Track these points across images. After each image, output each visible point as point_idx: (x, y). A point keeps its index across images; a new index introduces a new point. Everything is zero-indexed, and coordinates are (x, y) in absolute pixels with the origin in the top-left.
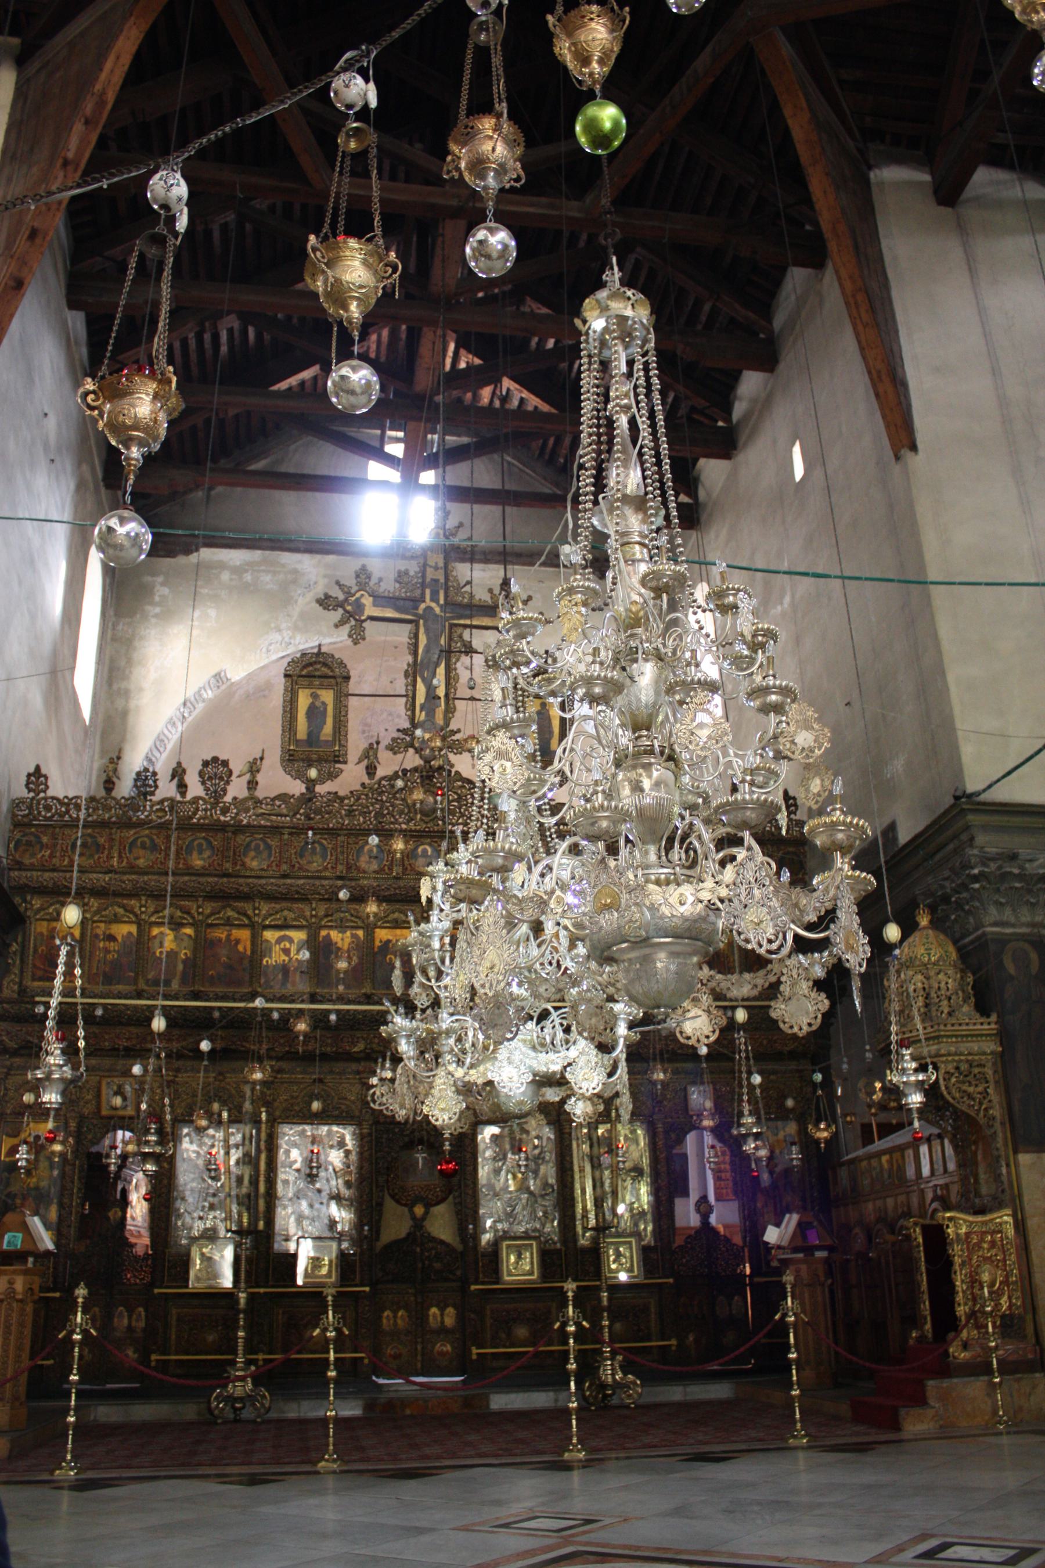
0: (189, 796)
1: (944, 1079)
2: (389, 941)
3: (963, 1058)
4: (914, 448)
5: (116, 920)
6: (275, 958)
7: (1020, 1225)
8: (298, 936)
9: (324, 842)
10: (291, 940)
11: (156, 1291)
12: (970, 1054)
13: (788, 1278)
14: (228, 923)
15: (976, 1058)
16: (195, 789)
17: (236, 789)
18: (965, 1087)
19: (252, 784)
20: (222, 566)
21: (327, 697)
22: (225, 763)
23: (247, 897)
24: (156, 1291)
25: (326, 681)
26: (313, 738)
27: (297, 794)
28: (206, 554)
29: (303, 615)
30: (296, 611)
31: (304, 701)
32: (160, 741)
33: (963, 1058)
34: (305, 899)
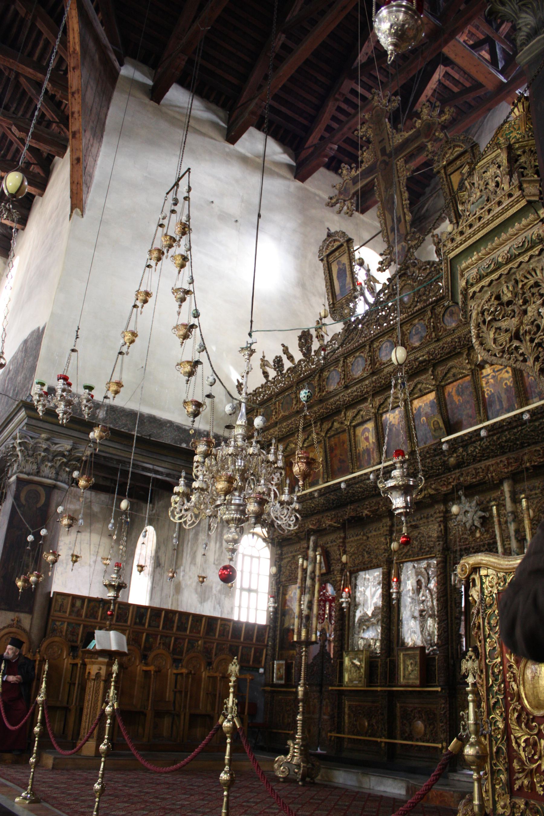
0: (296, 361)
1: (478, 325)
2: (420, 407)
3: (495, 276)
9: (362, 354)
10: (367, 430)
11: (330, 688)
12: (499, 266)
13: (234, 666)
15: (514, 264)
17: (315, 345)
18: (504, 324)
19: (320, 337)
23: (337, 411)
24: (330, 688)
25: (341, 250)
27: (341, 331)
33: (495, 276)
34: (365, 400)
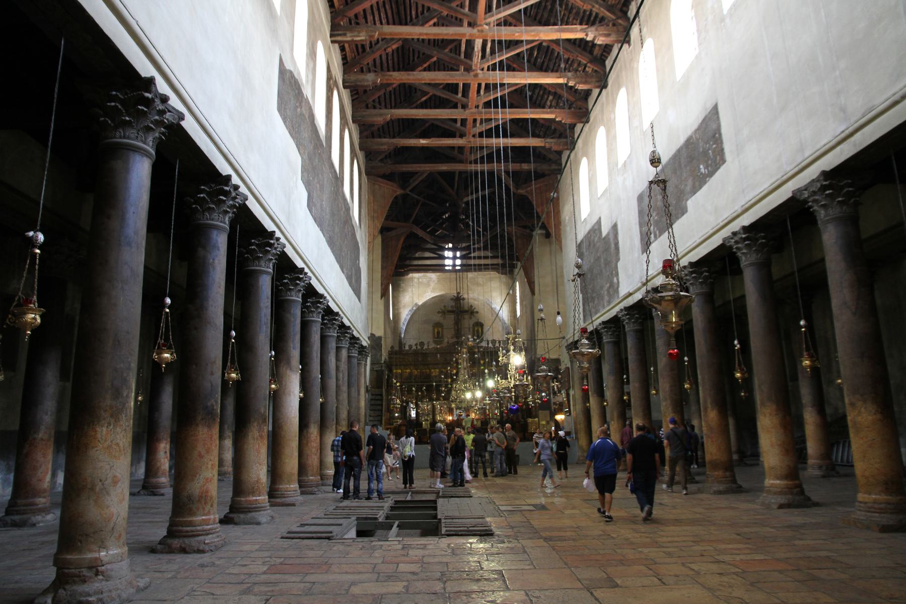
4: (534, 295)
5: (407, 369)
6: (434, 374)
7: (539, 421)
8: (437, 370)
14: (425, 369)
16: (419, 347)
17: (425, 347)
20: (415, 278)
21: (440, 329)
26: (438, 337)
28: (411, 275)
29: (433, 288)
30: (431, 287)
31: (436, 331)
32: (405, 319)
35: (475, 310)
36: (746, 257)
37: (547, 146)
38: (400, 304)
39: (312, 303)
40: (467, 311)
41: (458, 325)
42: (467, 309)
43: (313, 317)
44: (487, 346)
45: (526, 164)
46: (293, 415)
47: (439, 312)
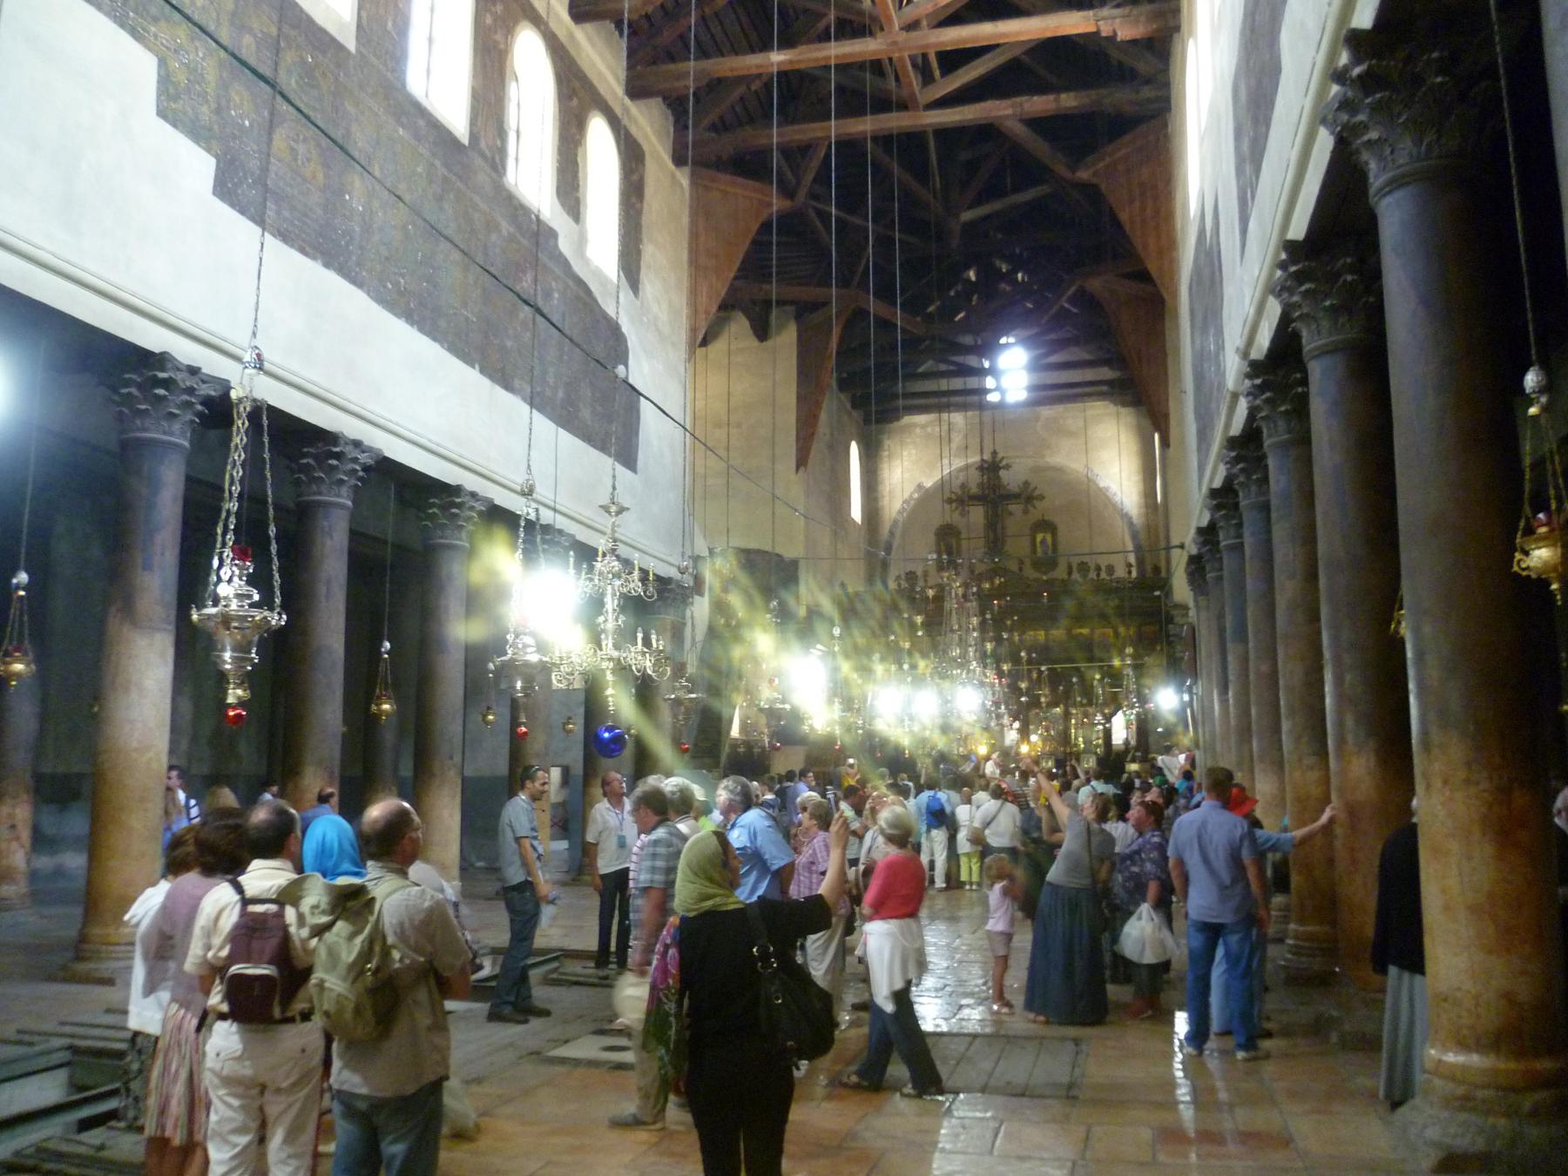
20: (915, 425)
22: (914, 573)
28: (907, 419)
32: (895, 522)
35: (1037, 493)
36: (1381, 159)
37: (1106, 31)
38: (880, 488)
39: (316, 457)
40: (1017, 496)
41: (995, 531)
42: (1017, 490)
43: (320, 493)
44: (1065, 576)
45: (1072, 94)
46: (135, 744)
47: (950, 501)
